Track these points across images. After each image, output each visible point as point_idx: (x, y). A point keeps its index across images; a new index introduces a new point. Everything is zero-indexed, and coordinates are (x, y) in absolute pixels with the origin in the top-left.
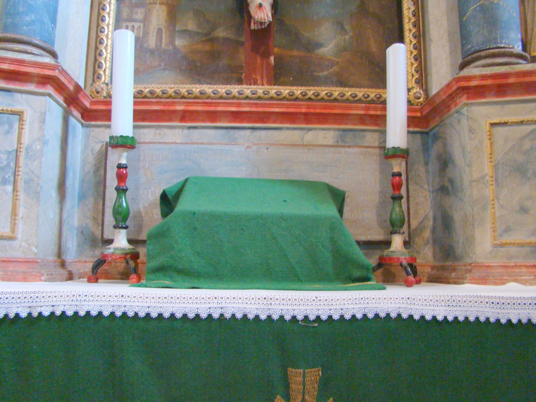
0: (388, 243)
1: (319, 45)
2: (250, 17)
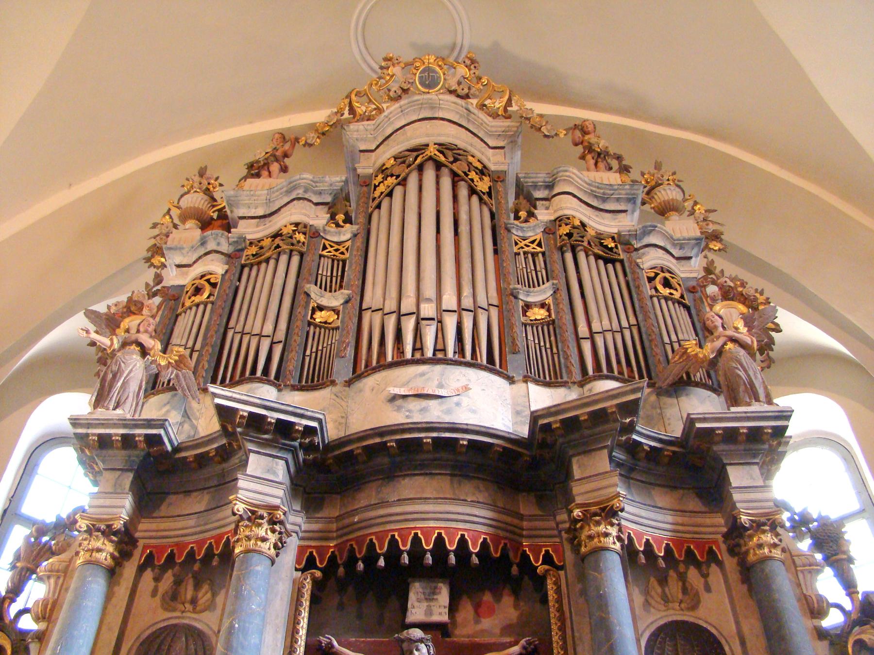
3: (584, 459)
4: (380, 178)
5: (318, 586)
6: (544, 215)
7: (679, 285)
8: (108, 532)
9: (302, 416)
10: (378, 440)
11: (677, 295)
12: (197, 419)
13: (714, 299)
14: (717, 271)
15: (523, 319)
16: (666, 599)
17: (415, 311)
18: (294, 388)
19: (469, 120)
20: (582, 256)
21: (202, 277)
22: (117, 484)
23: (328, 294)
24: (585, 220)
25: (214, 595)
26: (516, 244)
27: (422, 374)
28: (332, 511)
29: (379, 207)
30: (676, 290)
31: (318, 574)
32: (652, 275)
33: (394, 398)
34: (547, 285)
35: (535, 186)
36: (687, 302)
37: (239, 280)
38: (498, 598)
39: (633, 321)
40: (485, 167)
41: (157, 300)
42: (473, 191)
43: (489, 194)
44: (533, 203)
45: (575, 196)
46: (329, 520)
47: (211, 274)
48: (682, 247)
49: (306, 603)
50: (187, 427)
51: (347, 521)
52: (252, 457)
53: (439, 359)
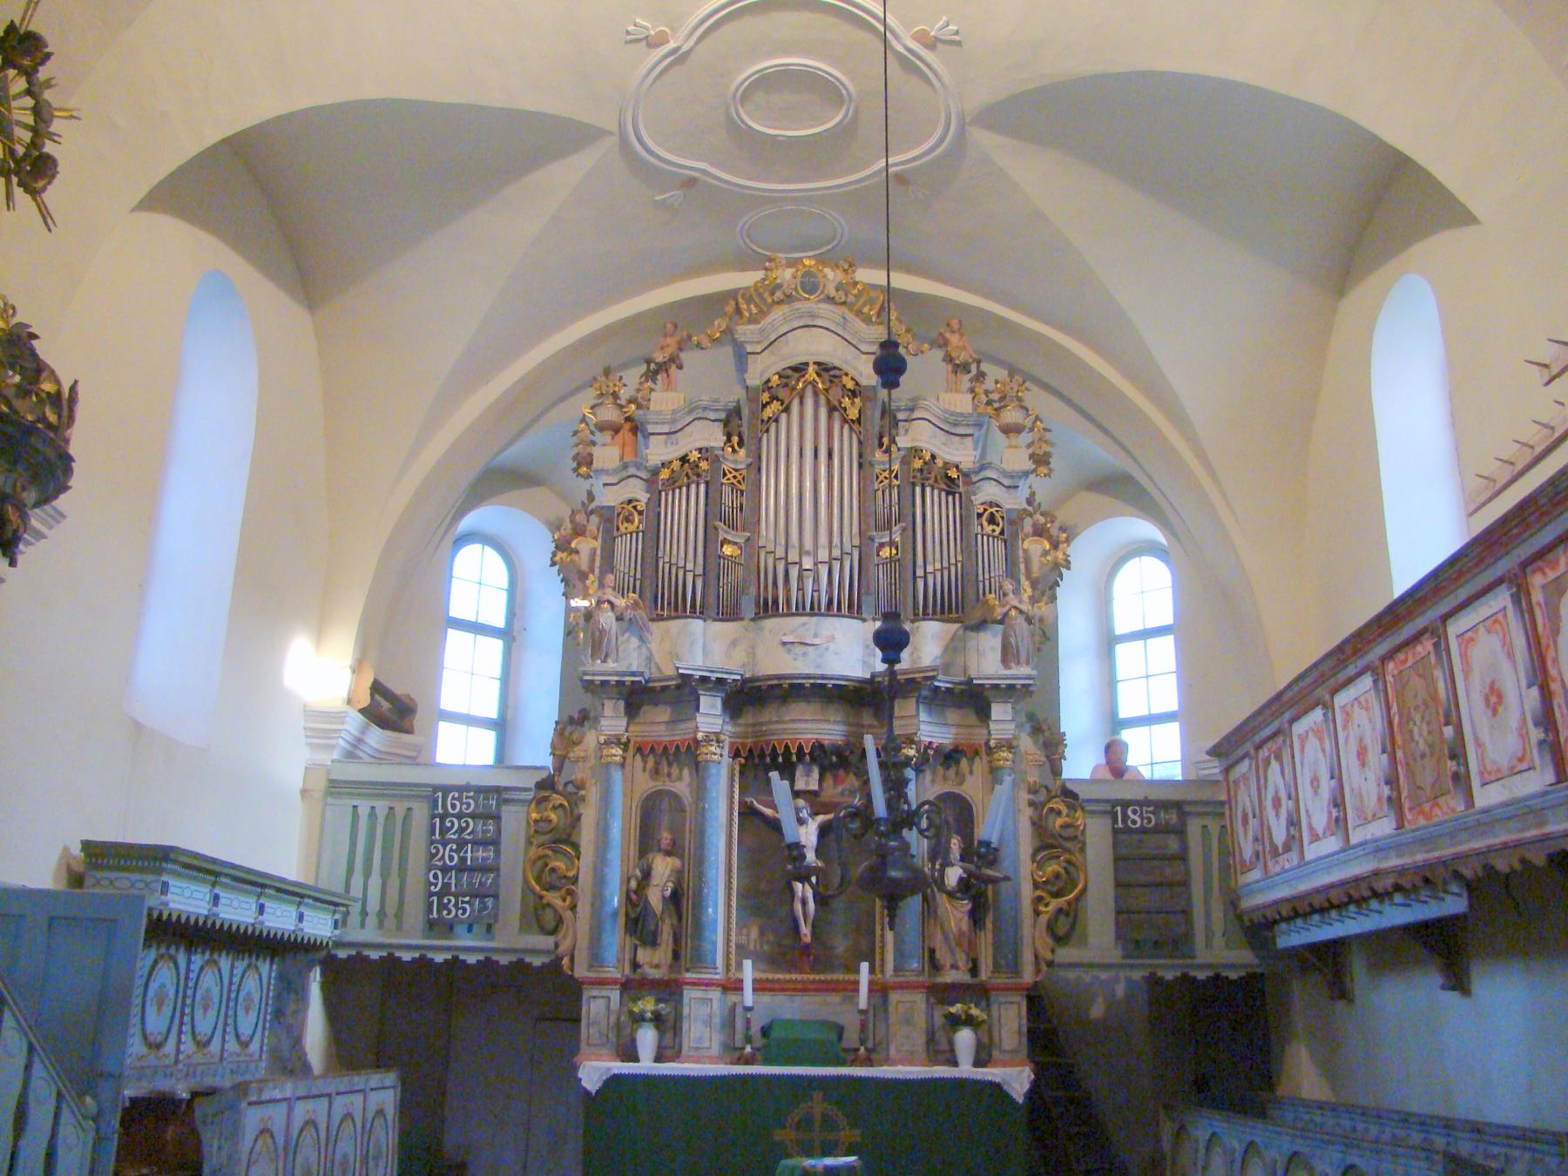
0: (857, 1050)
1: (836, 948)
2: (800, 939)
3: (902, 701)
4: (765, 397)
5: (742, 766)
6: (903, 441)
7: (1003, 518)
8: (618, 743)
9: (731, 673)
10: (776, 682)
11: (998, 530)
12: (650, 643)
13: (1027, 536)
14: (1036, 504)
15: (876, 560)
16: (945, 778)
17: (797, 560)
18: (715, 620)
19: (845, 329)
20: (928, 490)
21: (630, 502)
22: (615, 709)
23: (734, 532)
24: (936, 451)
25: (681, 771)
26: (877, 477)
27: (804, 624)
28: (748, 718)
29: (767, 431)
30: (998, 525)
31: (743, 761)
32: (981, 511)
33: (784, 644)
34: (898, 526)
35: (899, 410)
36: (1005, 537)
37: (659, 505)
38: (848, 774)
39: (959, 558)
40: (857, 384)
41: (594, 519)
42: (845, 421)
43: (859, 420)
44: (895, 423)
45: (930, 421)
46: (747, 725)
47: (637, 501)
48: (1012, 477)
49: (737, 779)
50: (644, 650)
51: (758, 728)
52: (702, 699)
53: (814, 611)
